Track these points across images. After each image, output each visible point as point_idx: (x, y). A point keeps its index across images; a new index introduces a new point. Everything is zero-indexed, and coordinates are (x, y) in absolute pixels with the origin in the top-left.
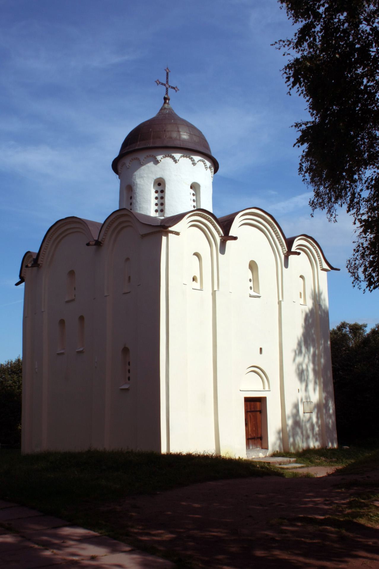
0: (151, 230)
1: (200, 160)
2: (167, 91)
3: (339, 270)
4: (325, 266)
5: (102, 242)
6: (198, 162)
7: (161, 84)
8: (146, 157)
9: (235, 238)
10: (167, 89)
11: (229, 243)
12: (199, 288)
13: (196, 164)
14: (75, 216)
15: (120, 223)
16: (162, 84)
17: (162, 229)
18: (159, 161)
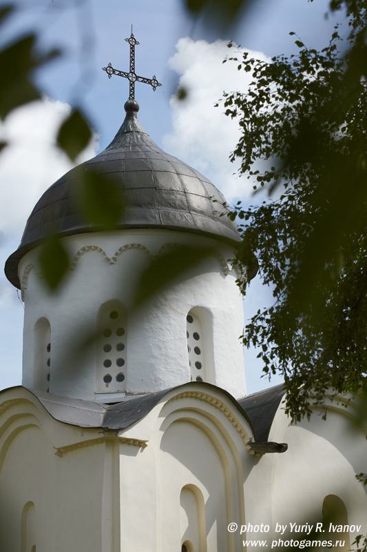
0: (77, 438)
2: (133, 88)
7: (118, 75)
9: (281, 448)
10: (132, 84)
16: (120, 74)
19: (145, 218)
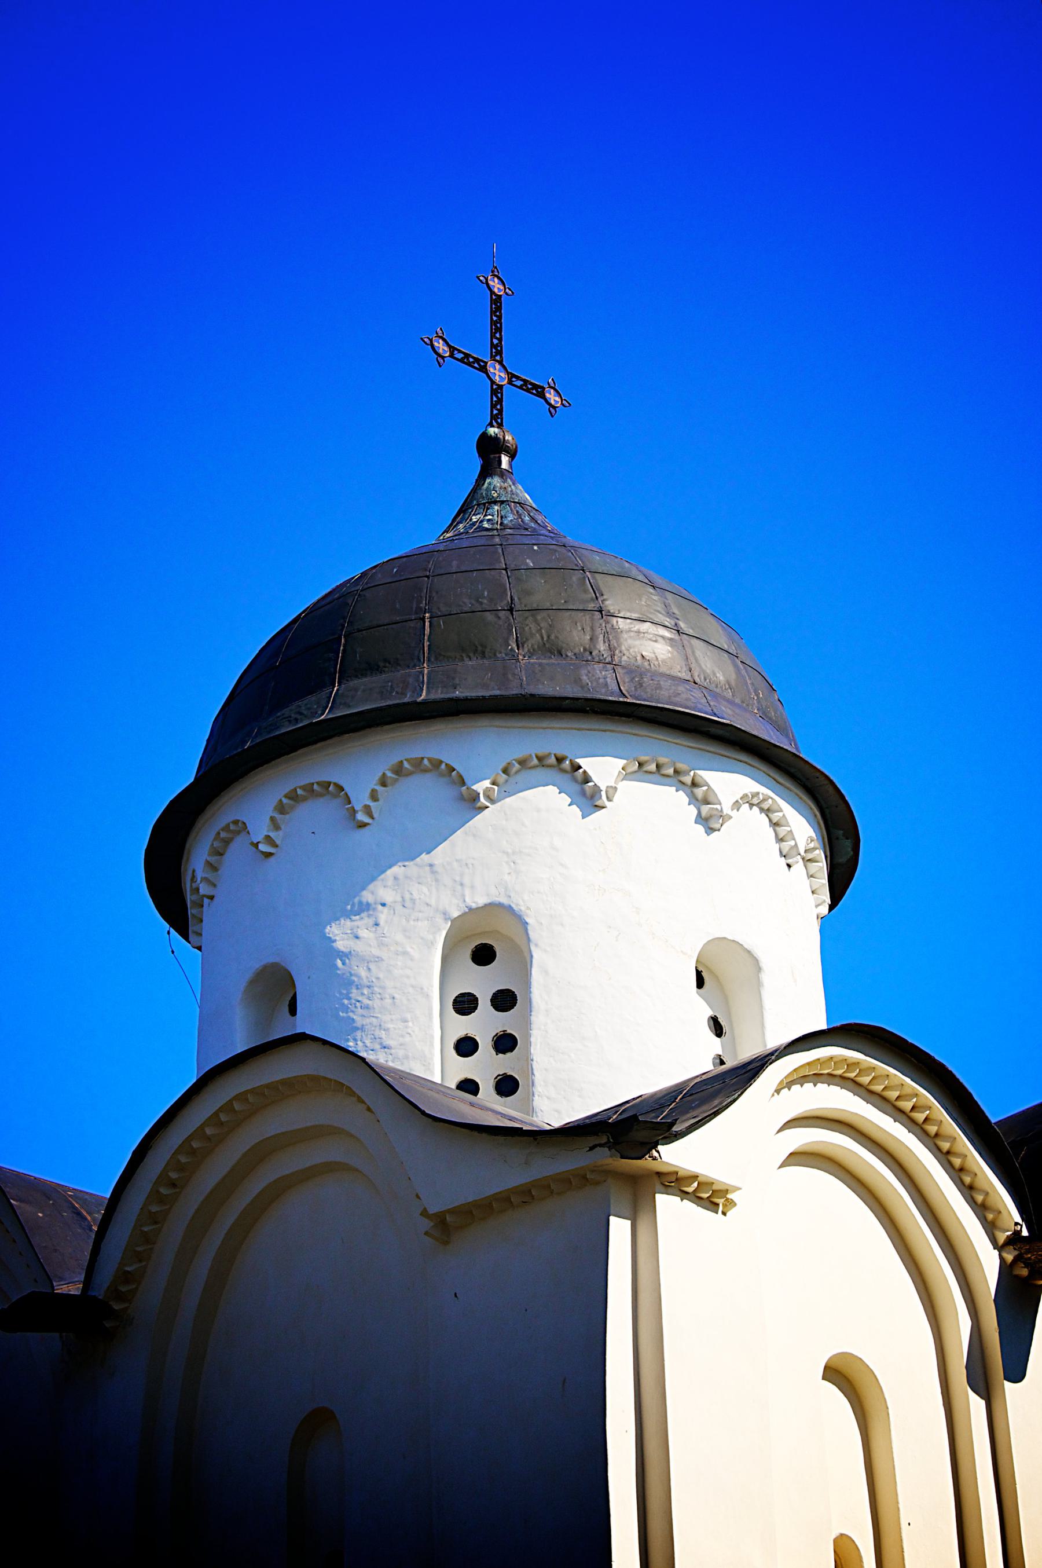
1: (750, 801)
2: (500, 401)
5: (116, 1306)
6: (737, 806)
7: (461, 360)
10: (497, 390)
13: (725, 818)
16: (466, 359)
17: (608, 1159)
19: (578, 681)
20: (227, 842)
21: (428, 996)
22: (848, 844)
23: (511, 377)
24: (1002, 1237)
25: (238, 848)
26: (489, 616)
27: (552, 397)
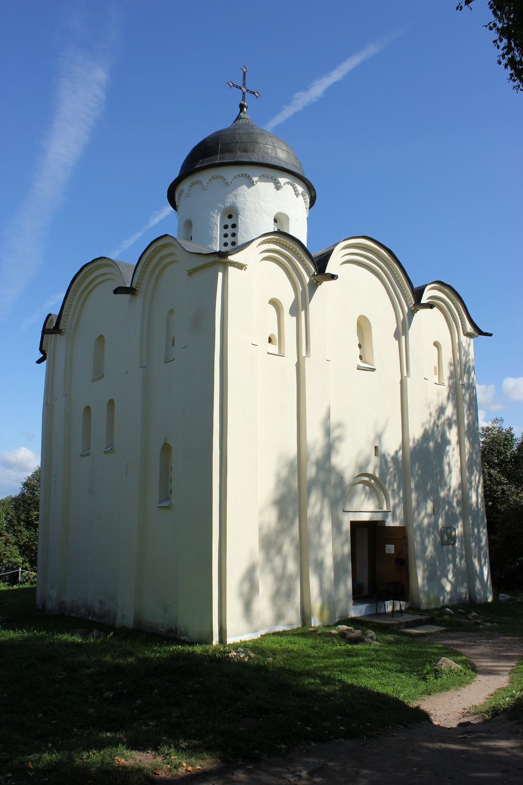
1: (288, 183)
3: (491, 335)
4: (469, 328)
6: (284, 184)
8: (211, 179)
9: (333, 277)
10: (244, 93)
11: (326, 285)
12: (277, 352)
14: (103, 256)
15: (162, 259)
16: (237, 87)
17: (217, 258)
18: (229, 183)
19: (250, 158)
20: (181, 194)
21: (217, 225)
22: (313, 192)
23: (247, 90)
24: (311, 274)
25: (183, 195)
26: (233, 144)
27: (257, 94)
